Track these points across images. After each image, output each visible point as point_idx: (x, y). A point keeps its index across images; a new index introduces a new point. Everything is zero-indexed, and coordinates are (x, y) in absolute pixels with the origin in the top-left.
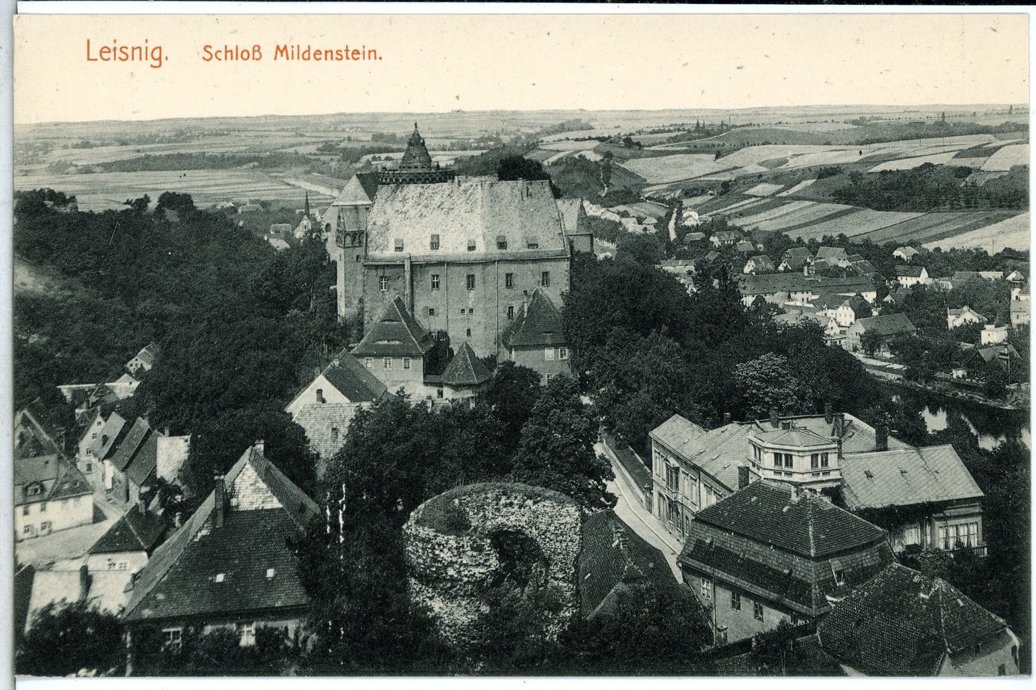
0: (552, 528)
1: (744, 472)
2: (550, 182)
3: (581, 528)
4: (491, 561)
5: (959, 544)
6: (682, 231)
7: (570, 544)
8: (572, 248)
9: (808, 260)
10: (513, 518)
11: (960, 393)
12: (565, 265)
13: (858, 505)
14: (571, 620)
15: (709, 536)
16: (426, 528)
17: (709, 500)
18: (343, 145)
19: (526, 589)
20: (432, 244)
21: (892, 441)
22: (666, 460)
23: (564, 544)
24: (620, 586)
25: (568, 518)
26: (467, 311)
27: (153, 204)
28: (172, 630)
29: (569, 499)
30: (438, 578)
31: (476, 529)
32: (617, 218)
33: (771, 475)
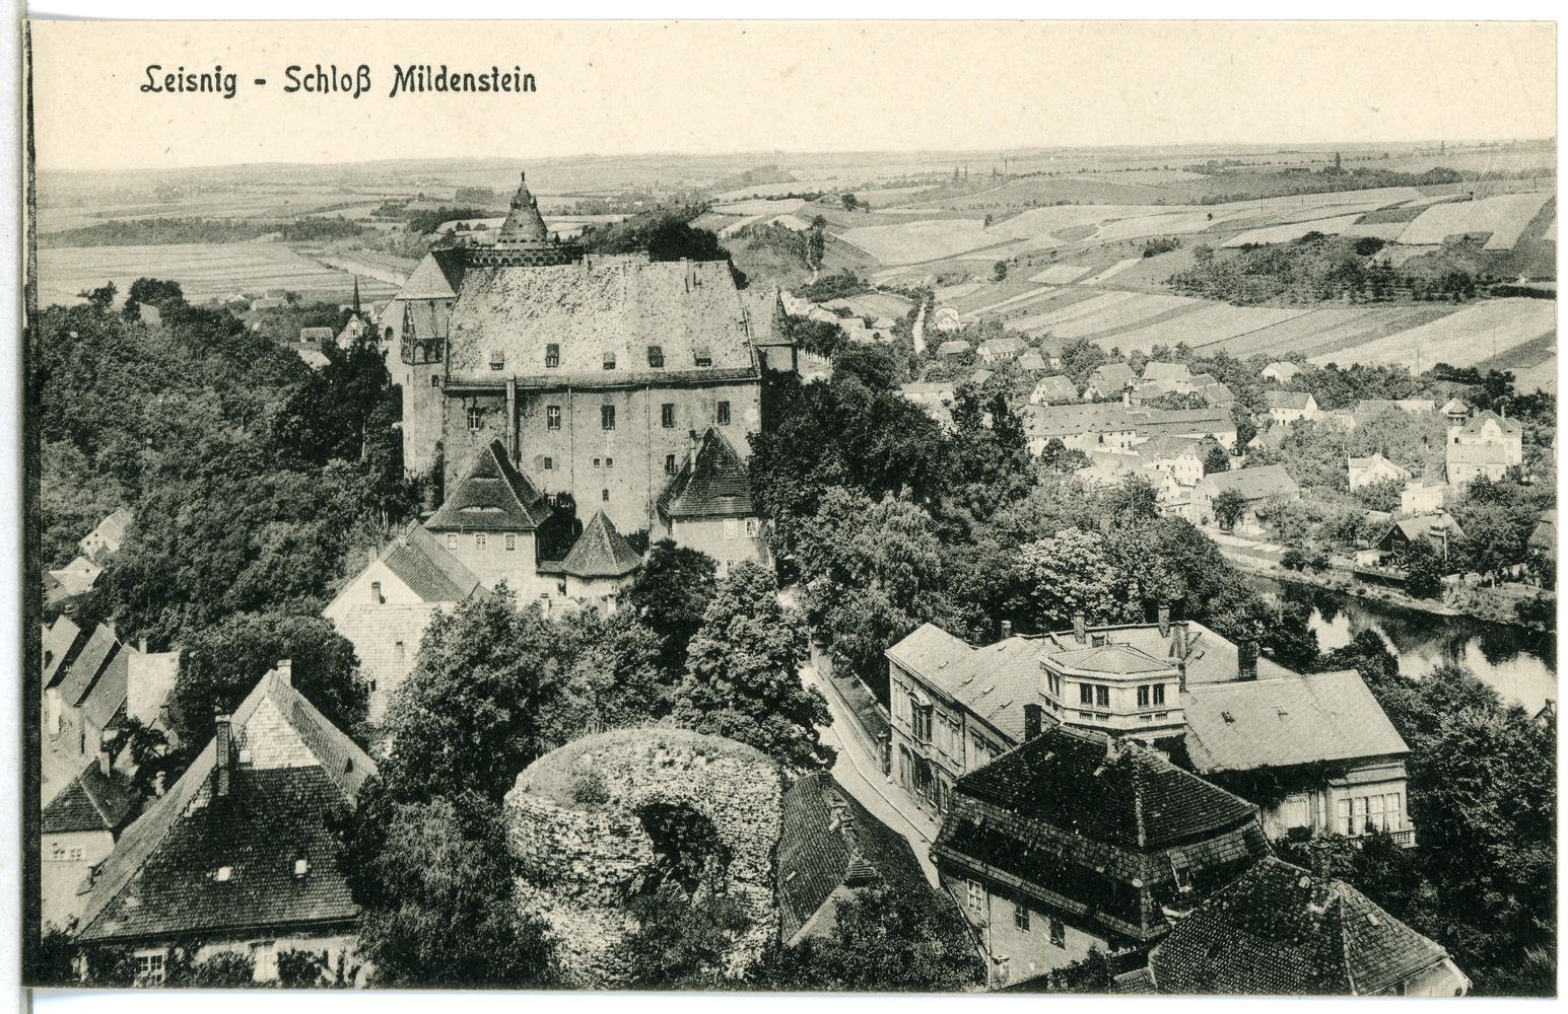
0: (735, 801)
1: (1033, 711)
2: (730, 264)
3: (781, 800)
4: (640, 852)
5: (1369, 827)
6: (936, 340)
7: (763, 825)
8: (764, 365)
9: (1130, 384)
10: (674, 785)
11: (1368, 590)
12: (753, 392)
13: (1212, 766)
14: (765, 945)
15: (977, 812)
16: (541, 800)
17: (978, 759)
18: (411, 206)
19: (696, 895)
20: (549, 358)
21: (1264, 666)
22: (911, 694)
23: (754, 826)
24: (843, 893)
25: (760, 786)
26: (603, 462)
27: (120, 301)
28: (149, 953)
29: (763, 756)
30: (559, 877)
31: (616, 802)
32: (833, 319)
33: (1075, 718)
